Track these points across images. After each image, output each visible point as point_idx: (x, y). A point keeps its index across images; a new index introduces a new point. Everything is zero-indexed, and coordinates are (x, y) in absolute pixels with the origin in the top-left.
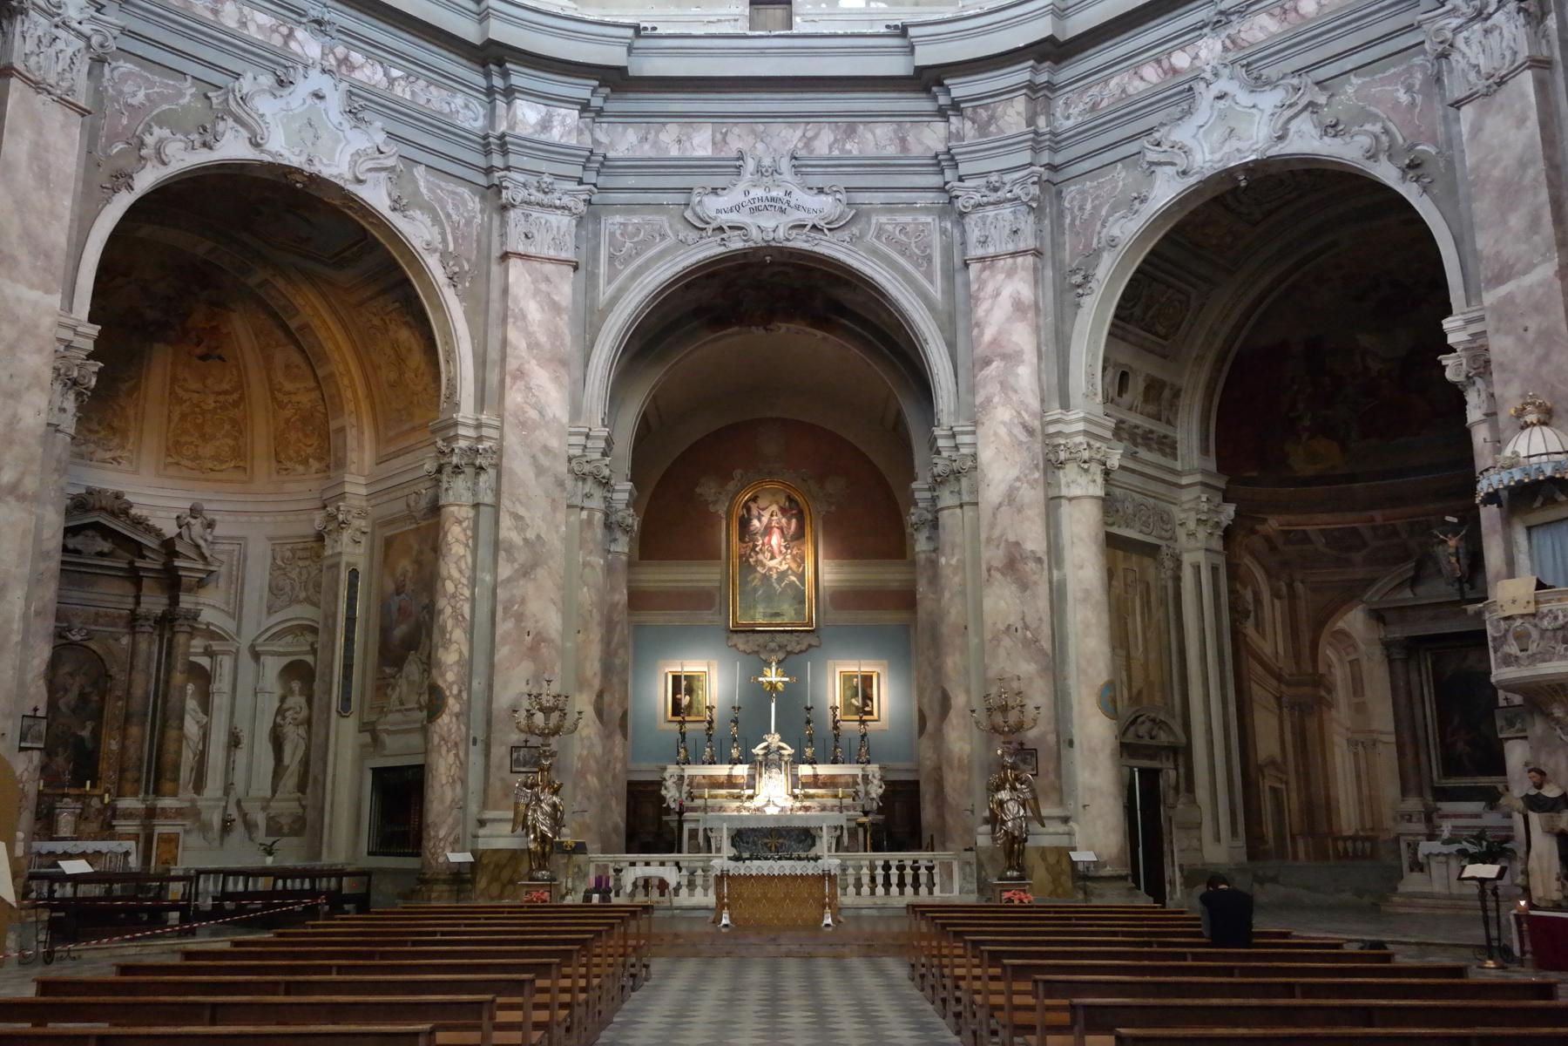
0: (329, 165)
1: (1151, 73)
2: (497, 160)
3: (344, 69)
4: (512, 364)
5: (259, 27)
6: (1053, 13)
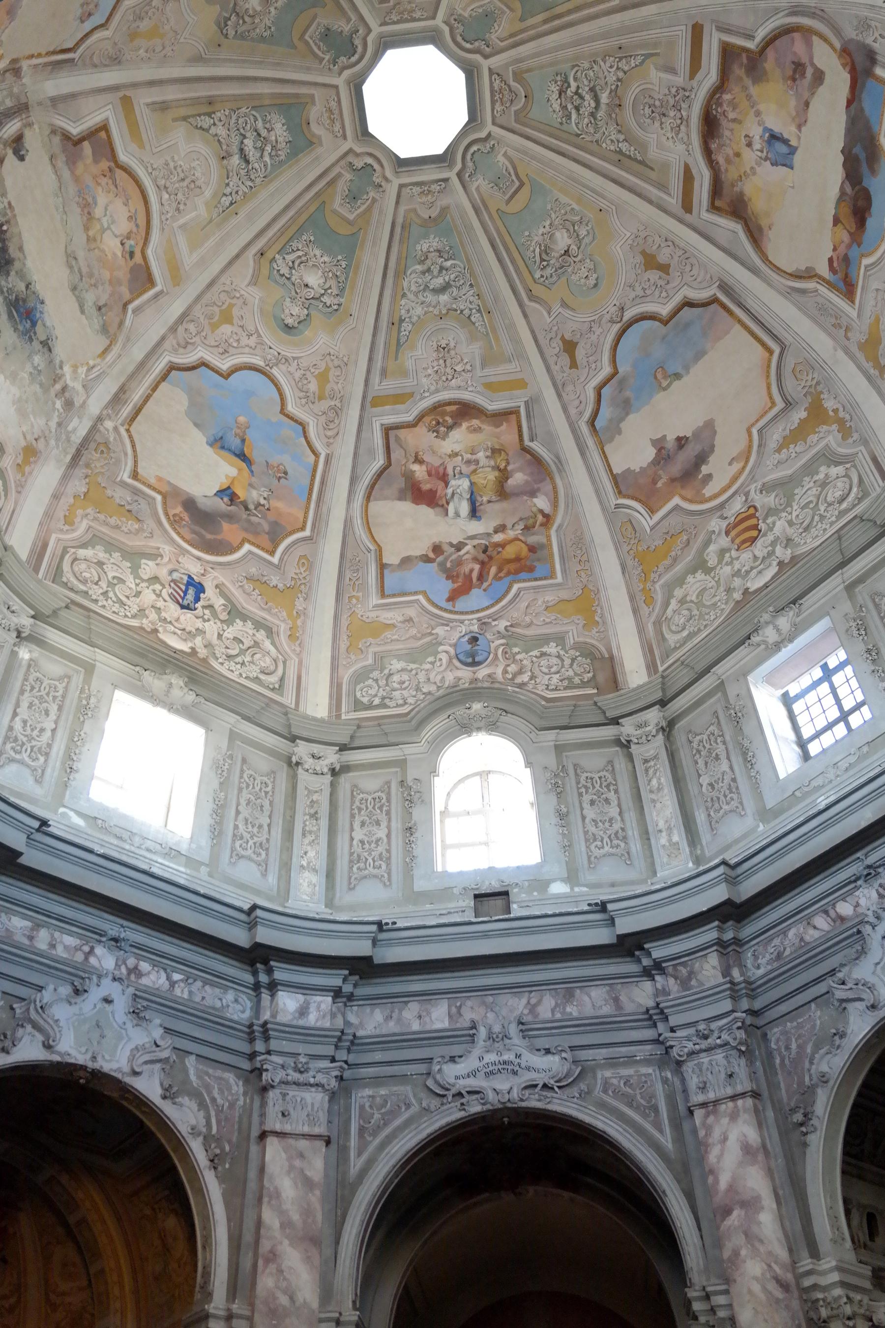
0: (110, 1061)
1: (821, 922)
2: (260, 1046)
3: (133, 977)
4: (265, 1246)
5: (66, 948)
6: (726, 881)
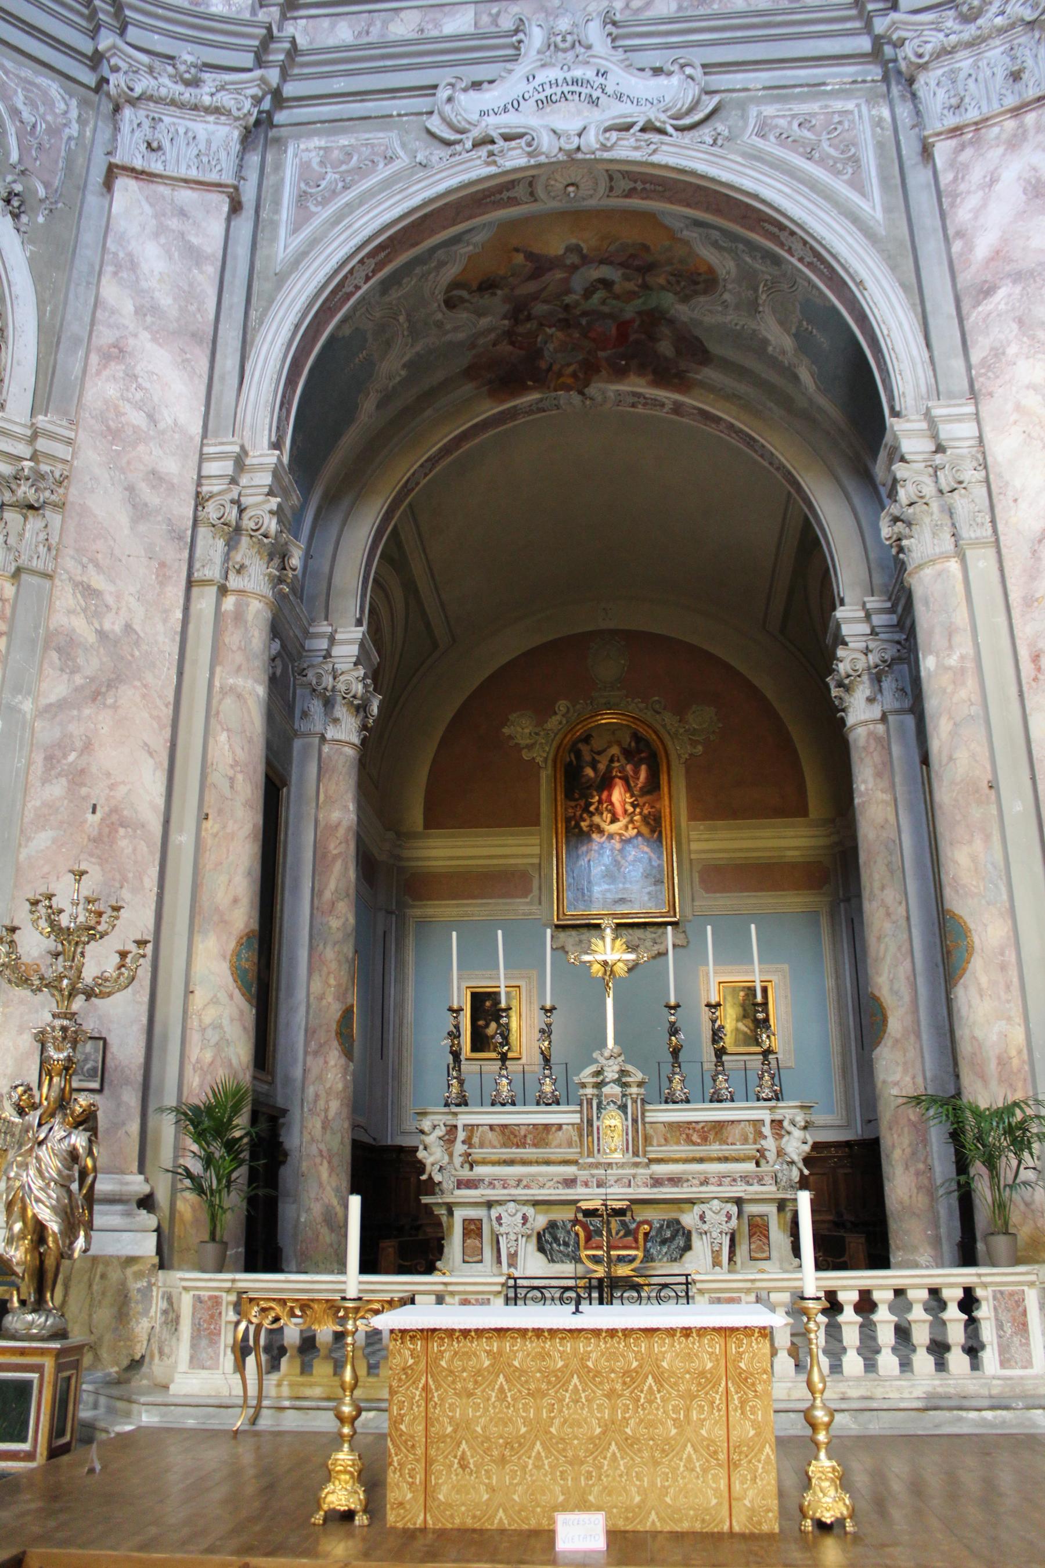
4: (105, 336)
